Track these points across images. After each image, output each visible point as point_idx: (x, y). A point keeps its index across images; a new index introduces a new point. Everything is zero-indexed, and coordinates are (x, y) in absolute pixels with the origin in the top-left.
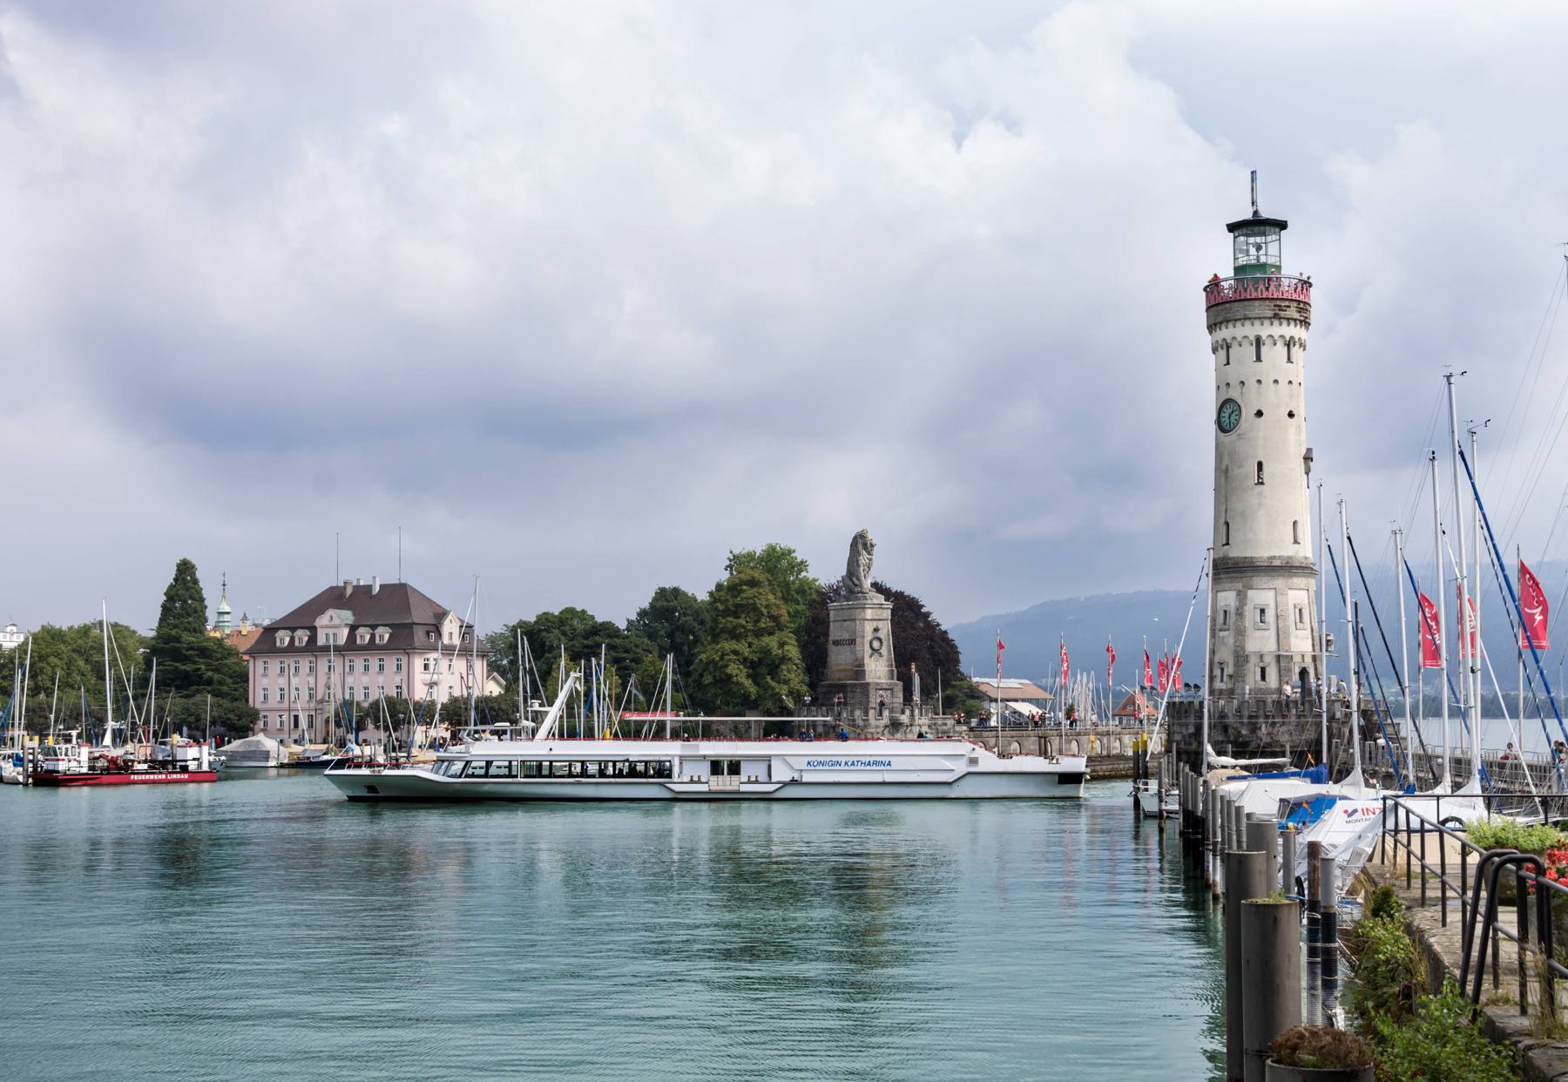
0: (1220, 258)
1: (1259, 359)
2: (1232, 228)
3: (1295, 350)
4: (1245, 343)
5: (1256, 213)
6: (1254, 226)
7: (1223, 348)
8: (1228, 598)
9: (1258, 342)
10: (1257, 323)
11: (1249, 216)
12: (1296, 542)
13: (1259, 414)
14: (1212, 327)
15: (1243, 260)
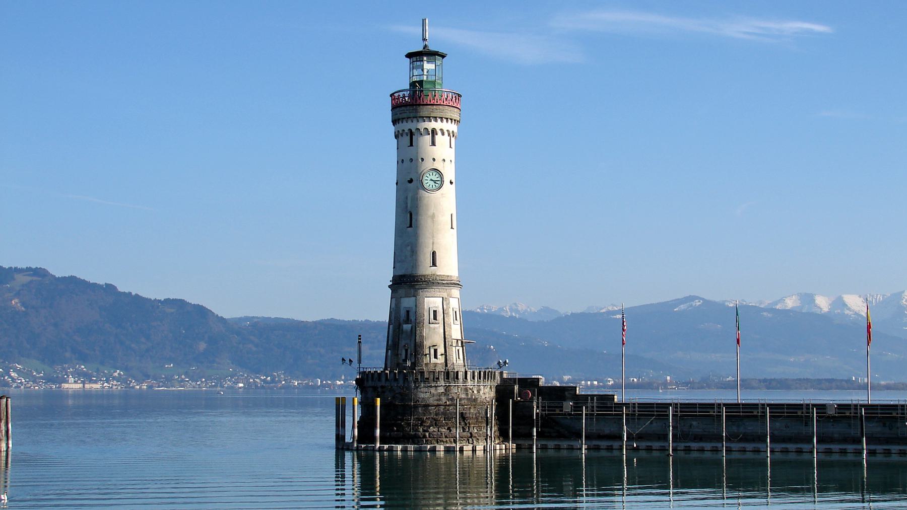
0: (400, 80)
1: (411, 145)
2: (409, 56)
3: (438, 137)
4: (405, 135)
5: (425, 46)
6: (415, 57)
7: (396, 137)
8: (407, 303)
9: (411, 134)
10: (420, 120)
11: (421, 49)
12: (434, 264)
13: (411, 181)
14: (394, 122)
15: (415, 79)
